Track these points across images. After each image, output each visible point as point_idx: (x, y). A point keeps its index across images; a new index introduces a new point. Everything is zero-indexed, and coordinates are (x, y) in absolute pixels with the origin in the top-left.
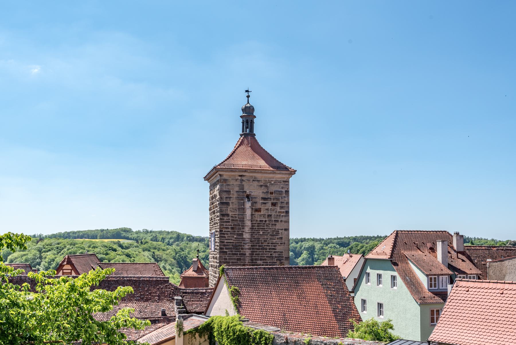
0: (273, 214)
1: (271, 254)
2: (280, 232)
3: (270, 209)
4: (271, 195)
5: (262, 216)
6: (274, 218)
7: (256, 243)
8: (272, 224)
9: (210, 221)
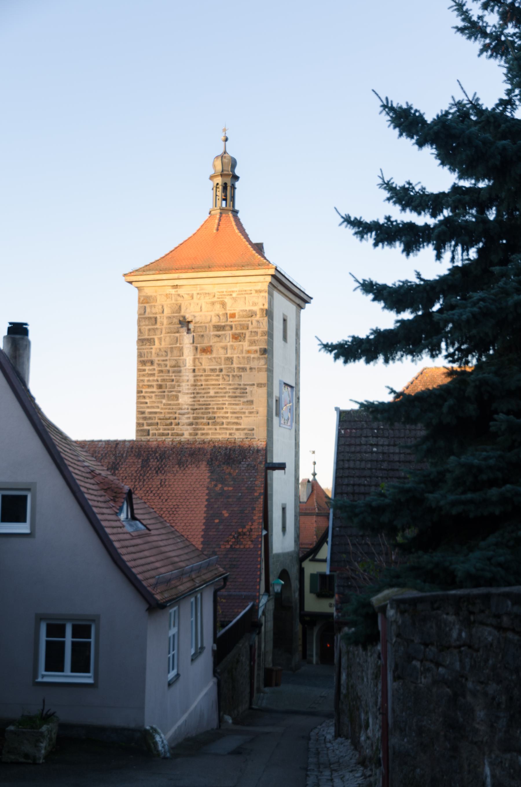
0: (235, 356)
1: (230, 434)
2: (247, 391)
4: (231, 320)
7: (202, 413)
8: (233, 376)
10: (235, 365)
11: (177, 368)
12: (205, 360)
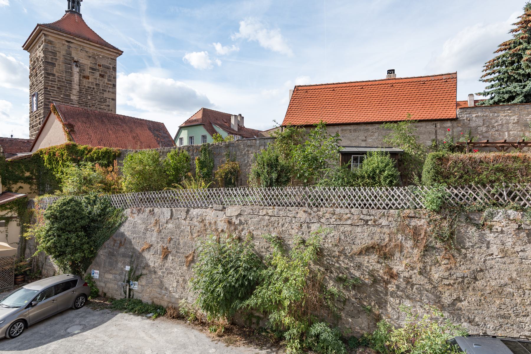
8: (100, 92)
9: (30, 87)
10: (101, 88)
11: (70, 82)
12: (85, 81)
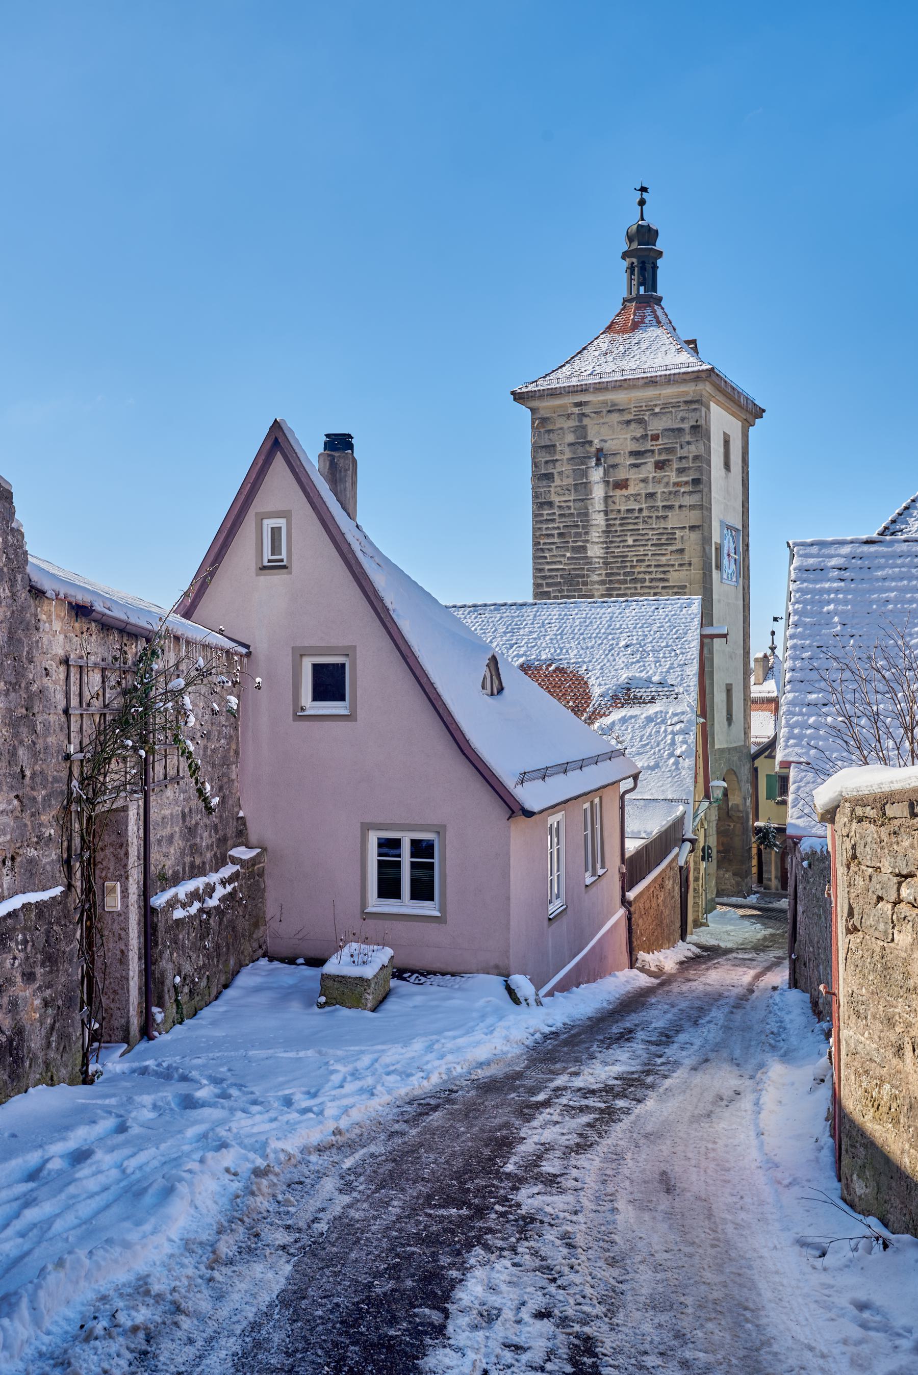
0: (659, 491)
3: (650, 479)
4: (654, 443)
5: (632, 499)
6: (662, 501)
7: (618, 568)
8: (657, 517)
